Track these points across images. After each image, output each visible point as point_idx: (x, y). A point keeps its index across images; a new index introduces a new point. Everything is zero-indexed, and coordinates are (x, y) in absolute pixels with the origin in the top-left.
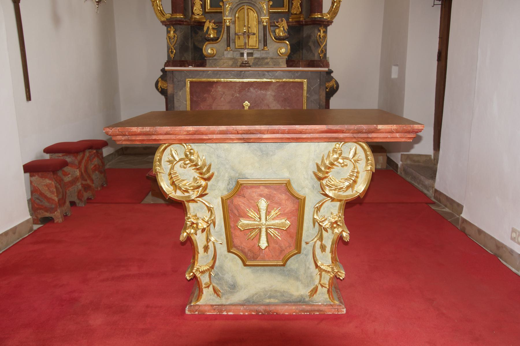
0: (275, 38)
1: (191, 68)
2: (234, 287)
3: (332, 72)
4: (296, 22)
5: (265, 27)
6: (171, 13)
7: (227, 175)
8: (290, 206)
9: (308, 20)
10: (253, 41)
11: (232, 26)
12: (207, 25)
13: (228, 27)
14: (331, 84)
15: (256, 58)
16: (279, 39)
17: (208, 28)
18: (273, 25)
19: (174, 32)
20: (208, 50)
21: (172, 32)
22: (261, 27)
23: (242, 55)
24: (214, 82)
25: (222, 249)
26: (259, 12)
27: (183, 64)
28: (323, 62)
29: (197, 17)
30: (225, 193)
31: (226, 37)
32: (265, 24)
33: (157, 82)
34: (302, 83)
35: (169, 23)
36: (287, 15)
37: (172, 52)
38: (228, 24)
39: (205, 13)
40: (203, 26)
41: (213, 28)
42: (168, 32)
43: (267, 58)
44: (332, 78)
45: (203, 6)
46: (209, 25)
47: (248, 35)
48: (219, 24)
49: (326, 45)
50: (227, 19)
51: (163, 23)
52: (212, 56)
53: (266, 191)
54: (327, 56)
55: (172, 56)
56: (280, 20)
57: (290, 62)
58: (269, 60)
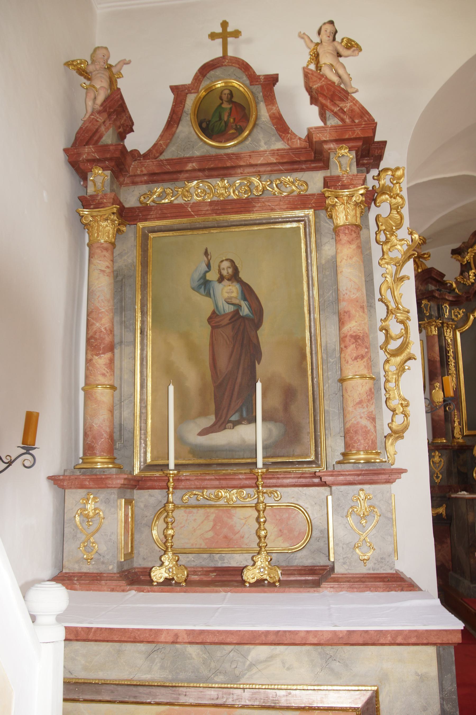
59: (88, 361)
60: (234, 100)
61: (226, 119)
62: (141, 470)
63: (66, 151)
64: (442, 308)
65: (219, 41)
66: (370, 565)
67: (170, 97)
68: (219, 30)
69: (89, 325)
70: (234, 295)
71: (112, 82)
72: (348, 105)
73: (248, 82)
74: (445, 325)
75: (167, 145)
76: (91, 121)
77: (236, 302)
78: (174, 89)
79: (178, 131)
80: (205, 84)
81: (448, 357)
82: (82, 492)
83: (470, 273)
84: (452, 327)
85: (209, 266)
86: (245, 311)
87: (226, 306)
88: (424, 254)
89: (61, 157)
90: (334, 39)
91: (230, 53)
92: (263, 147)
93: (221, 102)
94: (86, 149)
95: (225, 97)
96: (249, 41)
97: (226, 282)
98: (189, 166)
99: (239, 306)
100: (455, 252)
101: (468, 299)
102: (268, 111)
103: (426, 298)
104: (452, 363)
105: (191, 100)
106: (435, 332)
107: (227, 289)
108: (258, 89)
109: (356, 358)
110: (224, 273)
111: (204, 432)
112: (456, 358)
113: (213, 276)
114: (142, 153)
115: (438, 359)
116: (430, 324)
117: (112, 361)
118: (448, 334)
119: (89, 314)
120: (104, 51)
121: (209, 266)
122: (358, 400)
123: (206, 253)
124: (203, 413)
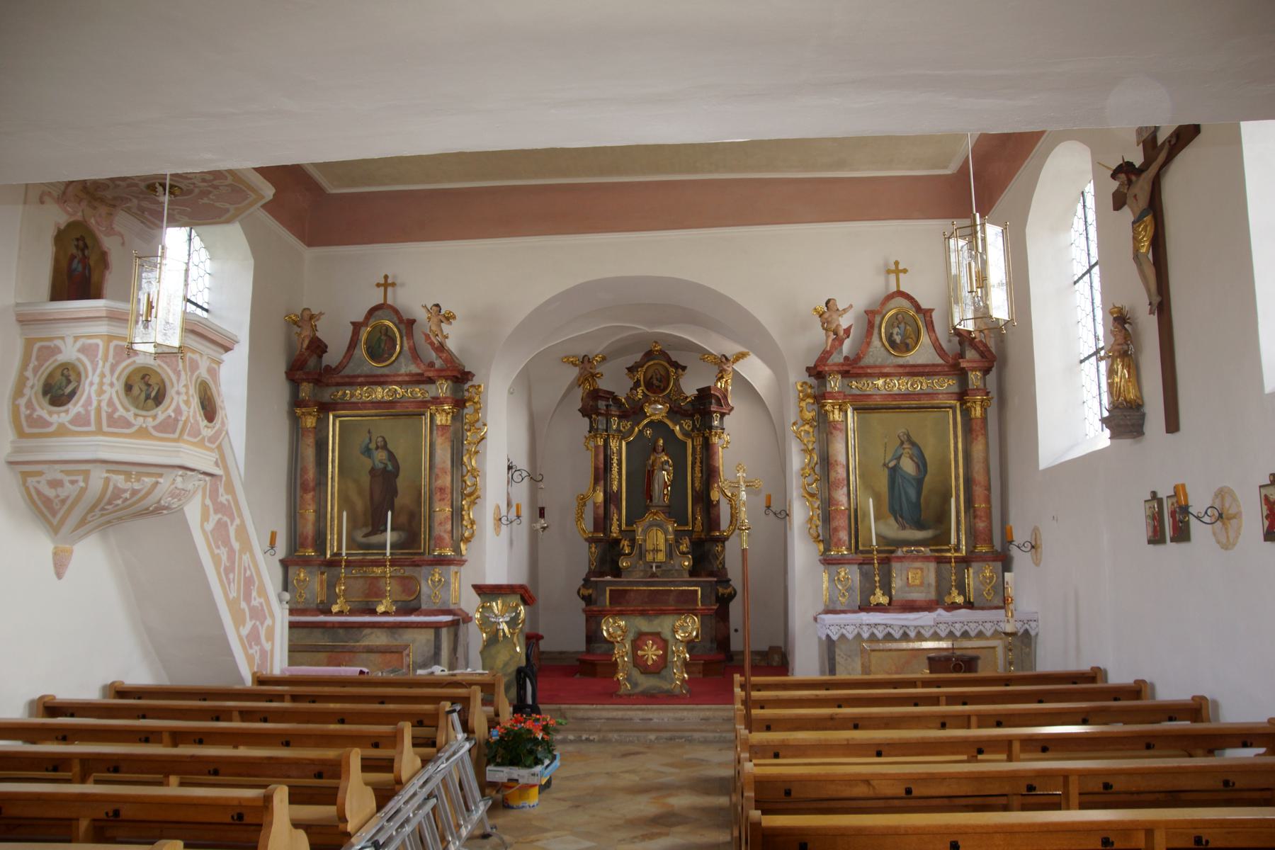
0: (680, 553)
1: (609, 578)
2: (635, 685)
3: (730, 580)
4: (698, 538)
5: (670, 545)
6: (592, 530)
7: (633, 630)
8: (662, 644)
9: (708, 537)
10: (661, 557)
11: (644, 544)
12: (623, 542)
13: (640, 545)
14: (729, 590)
15: (662, 570)
17: (624, 545)
18: (677, 542)
19: (596, 548)
21: (593, 549)
22: (668, 545)
23: (652, 567)
24: (628, 590)
25: (631, 665)
26: (666, 532)
27: (602, 574)
29: (615, 535)
30: (633, 638)
31: (638, 552)
32: (670, 542)
33: (579, 590)
34: (697, 591)
35: (590, 540)
37: (593, 564)
38: (640, 542)
39: (621, 531)
40: (620, 543)
41: (628, 546)
42: (590, 548)
43: (671, 570)
44: (731, 585)
45: (620, 526)
46: (625, 543)
47: (656, 551)
48: (633, 542)
49: (724, 558)
50: (639, 537)
51: (586, 540)
52: (627, 568)
53: (650, 637)
54: (726, 566)
55: (593, 567)
56: (683, 538)
57: (693, 572)
58: (674, 572)
59: (302, 497)
60: (388, 334)
61: (383, 346)
62: (331, 556)
63: (286, 373)
64: (610, 421)
65: (382, 289)
66: (438, 605)
67: (351, 327)
68: (382, 281)
69: (302, 476)
70: (384, 458)
71: (314, 329)
72: (445, 355)
73: (397, 322)
74: (611, 436)
75: (348, 363)
76: (301, 354)
77: (385, 462)
78: (353, 323)
79: (355, 352)
80: (372, 322)
82: (297, 568)
83: (638, 390)
84: (618, 438)
85: (370, 439)
86: (390, 467)
87: (379, 464)
88: (598, 374)
89: (284, 376)
90: (440, 312)
91: (390, 302)
92: (403, 371)
93: (380, 334)
94: (299, 372)
95: (383, 332)
96: (403, 285)
97: (380, 450)
98: (360, 380)
99: (386, 464)
100: (630, 370)
101: (634, 413)
102: (408, 343)
103: (594, 414)
105: (364, 334)
106: (600, 442)
107: (380, 454)
108: (402, 327)
109: (440, 500)
110: (379, 444)
111: (366, 536)
112: (620, 464)
113: (373, 446)
114: (333, 367)
115: (602, 466)
116: (595, 436)
117: (314, 497)
118: (614, 444)
119: (302, 469)
120: (308, 312)
121: (370, 439)
122: (439, 522)
123: (369, 432)
124: (365, 525)
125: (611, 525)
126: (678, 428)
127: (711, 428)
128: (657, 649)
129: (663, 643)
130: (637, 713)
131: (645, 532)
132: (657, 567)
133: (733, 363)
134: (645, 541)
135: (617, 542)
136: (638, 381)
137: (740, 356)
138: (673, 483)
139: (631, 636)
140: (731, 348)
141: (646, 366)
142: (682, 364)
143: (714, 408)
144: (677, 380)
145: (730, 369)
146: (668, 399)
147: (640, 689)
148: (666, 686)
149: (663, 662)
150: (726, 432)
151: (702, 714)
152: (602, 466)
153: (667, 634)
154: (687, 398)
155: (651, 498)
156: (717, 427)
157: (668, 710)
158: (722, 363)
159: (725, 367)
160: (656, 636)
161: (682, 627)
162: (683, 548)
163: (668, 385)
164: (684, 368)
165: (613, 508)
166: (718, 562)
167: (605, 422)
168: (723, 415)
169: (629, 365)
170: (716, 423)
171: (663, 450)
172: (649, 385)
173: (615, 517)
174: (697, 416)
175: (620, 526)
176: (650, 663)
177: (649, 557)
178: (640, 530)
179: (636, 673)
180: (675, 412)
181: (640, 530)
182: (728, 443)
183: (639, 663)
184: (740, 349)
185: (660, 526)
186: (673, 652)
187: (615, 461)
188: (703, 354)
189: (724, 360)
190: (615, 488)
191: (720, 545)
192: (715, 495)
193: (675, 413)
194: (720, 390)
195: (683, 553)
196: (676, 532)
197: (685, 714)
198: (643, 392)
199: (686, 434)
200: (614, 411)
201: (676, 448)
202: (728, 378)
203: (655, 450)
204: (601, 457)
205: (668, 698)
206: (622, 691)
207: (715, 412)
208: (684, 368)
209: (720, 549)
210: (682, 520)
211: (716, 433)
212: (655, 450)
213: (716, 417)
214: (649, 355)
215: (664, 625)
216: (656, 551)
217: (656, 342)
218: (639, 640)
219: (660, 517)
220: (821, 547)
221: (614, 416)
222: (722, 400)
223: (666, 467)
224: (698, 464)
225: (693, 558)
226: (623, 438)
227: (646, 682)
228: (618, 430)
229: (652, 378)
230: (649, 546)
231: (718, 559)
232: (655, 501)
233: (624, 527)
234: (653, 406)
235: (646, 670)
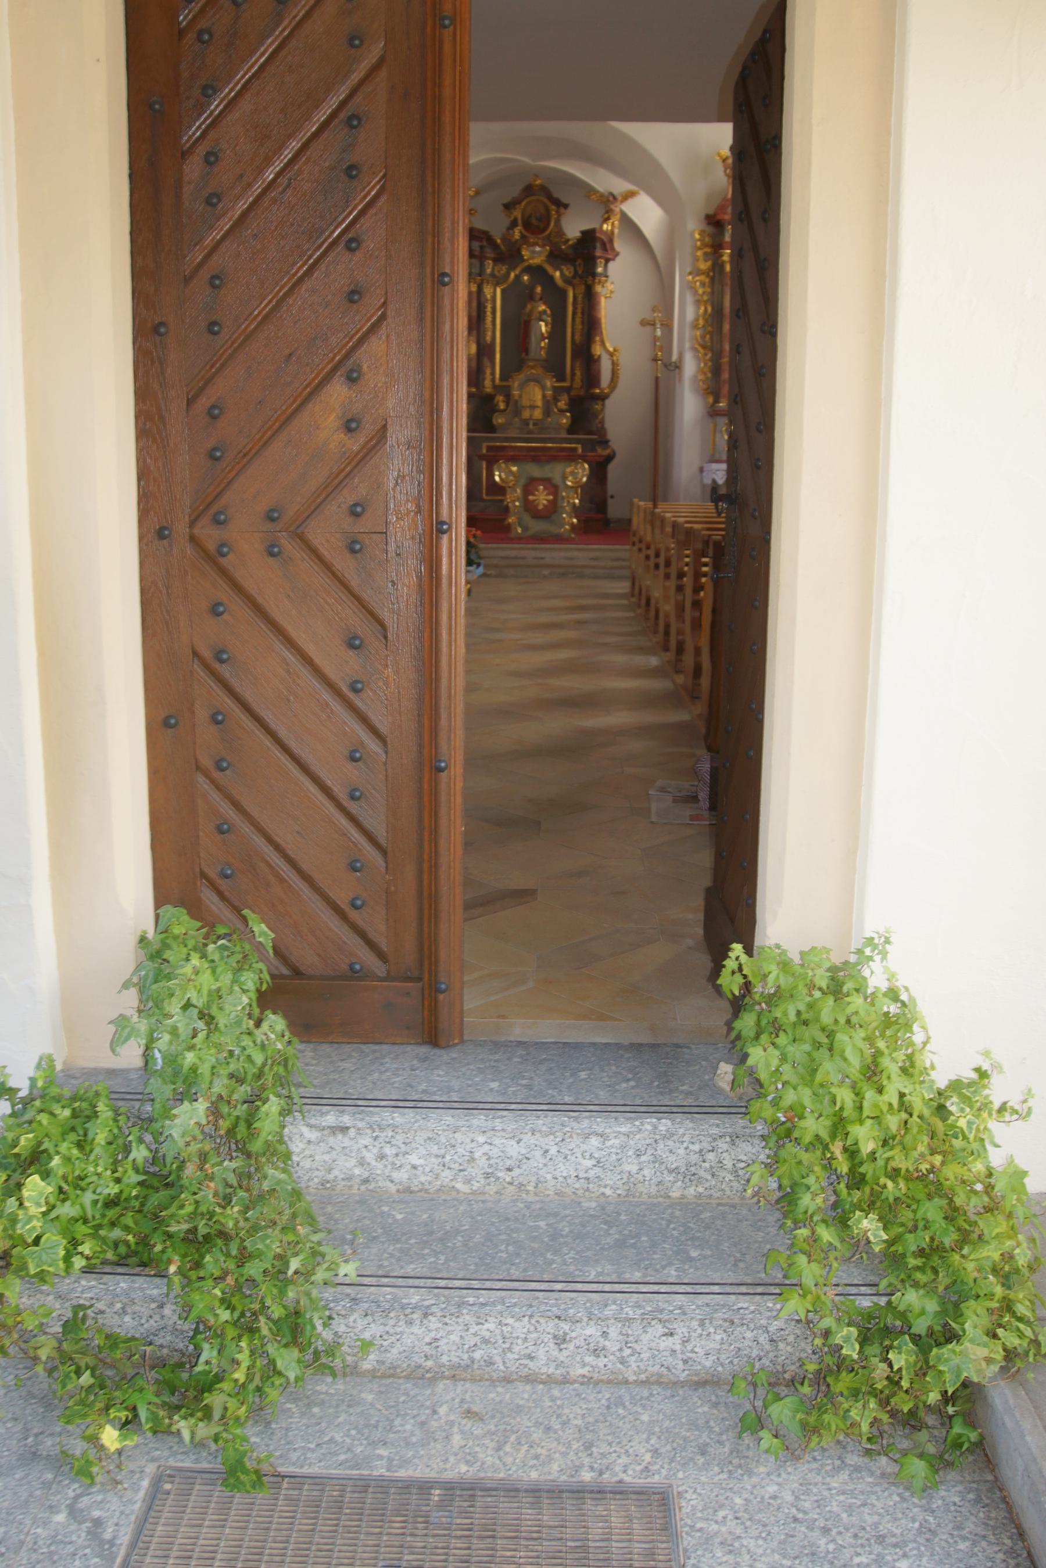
10: (538, 414)
16: (562, 411)
20: (499, 420)
26: (543, 388)
28: (602, 431)
36: (568, 390)
39: (495, 387)
45: (493, 380)
46: (500, 399)
48: (508, 397)
50: (516, 393)
57: (570, 431)
81: (485, 313)
100: (508, 207)
104: (489, 319)
112: (494, 312)
118: (488, 291)
125: (484, 379)
126: (558, 274)
127: (594, 275)
128: (548, 494)
129: (553, 488)
130: (530, 553)
131: (522, 387)
132: (535, 424)
133: (622, 202)
134: (520, 396)
135: (490, 398)
136: (516, 219)
137: (630, 195)
138: (551, 335)
139: (523, 481)
140: (618, 185)
141: (523, 204)
142: (565, 201)
143: (598, 252)
144: (558, 221)
145: (617, 210)
146: (548, 240)
147: (530, 533)
148: (554, 530)
149: (553, 508)
150: (610, 280)
151: (592, 554)
152: (474, 314)
153: (557, 479)
154: (568, 240)
155: (526, 350)
156: (600, 275)
157: (560, 550)
158: (607, 203)
159: (612, 207)
160: (547, 482)
161: (572, 473)
162: (562, 404)
163: (548, 225)
164: (566, 206)
165: (486, 362)
166: (597, 421)
167: (478, 265)
168: (607, 261)
169: (506, 200)
170: (600, 270)
171: (541, 299)
172: (527, 225)
173: (488, 371)
174: (579, 262)
175: (493, 380)
176: (541, 507)
177: (526, 414)
178: (516, 384)
179: (527, 519)
180: (556, 257)
181: (516, 384)
182: (612, 292)
183: (529, 507)
184: (630, 187)
185: (537, 381)
186: (563, 498)
187: (489, 309)
188: (589, 191)
189: (611, 198)
190: (488, 339)
191: (600, 403)
192: (597, 350)
193: (556, 257)
194: (606, 232)
195: (562, 411)
196: (555, 389)
197: (575, 554)
198: (521, 232)
199: (568, 281)
200: (489, 252)
201: (556, 297)
202: (616, 220)
203: (531, 297)
204: (474, 304)
205: (558, 539)
206: (512, 535)
207: (600, 257)
208: (566, 206)
209: (598, 407)
210: (561, 377)
211: (600, 282)
212: (531, 297)
213: (601, 262)
214: (529, 190)
215: (554, 471)
216: (533, 407)
217: (536, 176)
218: (529, 487)
219: (537, 371)
220: (711, 400)
221: (489, 258)
222: (607, 245)
223: (544, 317)
224: (579, 315)
225: (572, 416)
226: (498, 284)
227: (537, 527)
228: (493, 275)
229: (530, 217)
230: (525, 402)
231: (597, 417)
232: (532, 354)
233: (497, 381)
234: (531, 248)
235: (537, 515)
